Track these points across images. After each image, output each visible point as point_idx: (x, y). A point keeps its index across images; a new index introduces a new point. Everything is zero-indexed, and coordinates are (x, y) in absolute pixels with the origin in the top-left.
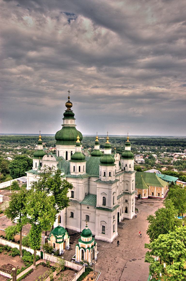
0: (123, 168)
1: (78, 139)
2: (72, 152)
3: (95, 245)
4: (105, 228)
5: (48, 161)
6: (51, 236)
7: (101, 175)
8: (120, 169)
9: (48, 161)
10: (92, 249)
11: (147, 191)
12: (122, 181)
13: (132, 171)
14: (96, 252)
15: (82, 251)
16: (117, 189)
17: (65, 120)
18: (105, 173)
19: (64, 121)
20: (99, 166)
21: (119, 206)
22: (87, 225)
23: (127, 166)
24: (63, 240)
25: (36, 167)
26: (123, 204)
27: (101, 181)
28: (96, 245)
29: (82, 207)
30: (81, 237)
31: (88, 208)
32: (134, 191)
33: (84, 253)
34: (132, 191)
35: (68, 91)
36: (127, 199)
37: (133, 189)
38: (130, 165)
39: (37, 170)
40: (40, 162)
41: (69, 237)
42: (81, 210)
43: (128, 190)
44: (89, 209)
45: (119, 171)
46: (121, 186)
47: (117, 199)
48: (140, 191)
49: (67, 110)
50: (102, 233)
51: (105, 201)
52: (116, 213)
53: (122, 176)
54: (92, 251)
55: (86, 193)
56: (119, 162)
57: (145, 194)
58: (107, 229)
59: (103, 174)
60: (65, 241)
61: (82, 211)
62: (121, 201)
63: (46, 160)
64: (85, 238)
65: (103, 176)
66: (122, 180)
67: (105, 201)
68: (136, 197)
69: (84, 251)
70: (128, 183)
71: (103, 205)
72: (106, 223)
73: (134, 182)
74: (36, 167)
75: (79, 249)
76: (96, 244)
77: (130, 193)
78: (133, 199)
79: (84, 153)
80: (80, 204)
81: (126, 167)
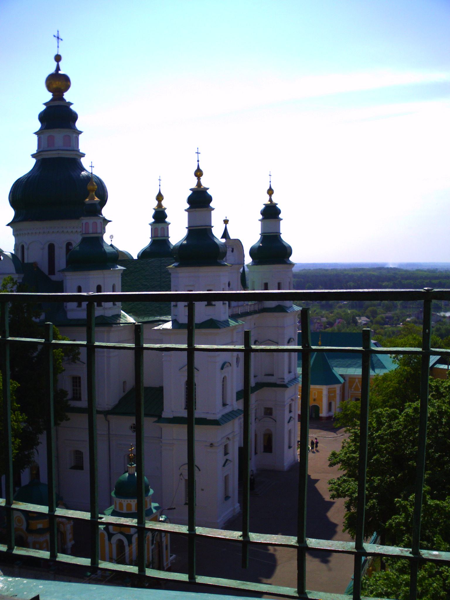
11: (338, 391)
14: (167, 549)
15: (120, 542)
26: (255, 423)
33: (127, 549)
35: (56, 34)
37: (290, 372)
43: (273, 375)
47: (237, 400)
49: (52, 100)
54: (155, 542)
57: (330, 405)
58: (203, 490)
64: (129, 500)
75: (110, 539)
77: (279, 382)
78: (290, 405)
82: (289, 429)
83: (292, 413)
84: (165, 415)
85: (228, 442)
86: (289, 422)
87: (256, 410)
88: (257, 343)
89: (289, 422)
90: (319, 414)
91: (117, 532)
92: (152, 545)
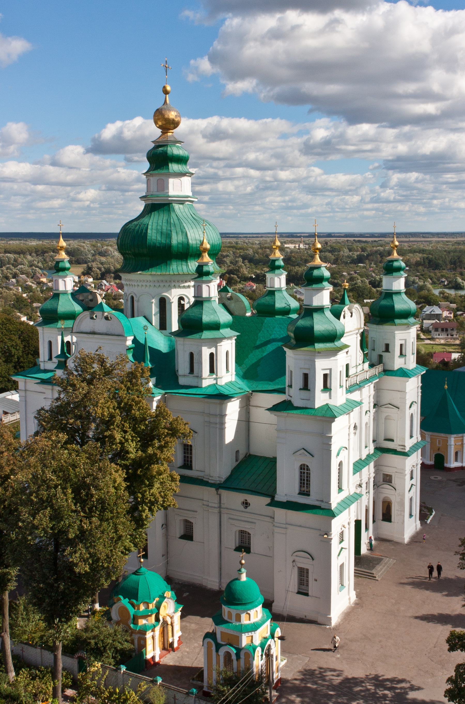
0: (375, 359)
1: (205, 250)
2: (181, 299)
3: (273, 636)
4: (307, 577)
5: (94, 333)
6: (115, 603)
7: (290, 386)
8: (363, 362)
9: (94, 333)
10: (263, 651)
12: (369, 407)
13: (411, 368)
15: (228, 655)
16: (352, 435)
17: (153, 180)
18: (306, 377)
19: (148, 182)
20: (285, 352)
21: (360, 495)
22: (242, 564)
23: (390, 349)
24: (157, 620)
25: (50, 359)
27: (292, 405)
28: (276, 635)
29: (222, 502)
30: (223, 606)
31: (247, 503)
32: (416, 442)
34: (409, 443)
36: (388, 471)
37: (411, 437)
38: (401, 345)
39: (56, 368)
40: (65, 341)
41: (180, 609)
42: (220, 513)
43: (392, 440)
44: (249, 509)
45: (360, 368)
46: (366, 424)
47: (354, 474)
48: (439, 441)
50: (299, 593)
51: (308, 481)
52: (349, 524)
53: (372, 386)
55: (237, 452)
56: (359, 335)
57: (456, 453)
58: (316, 580)
59: (298, 382)
60: (165, 623)
61: (222, 515)
62: (369, 479)
63: (88, 330)
65: (300, 389)
66: (372, 405)
67: (307, 480)
68: (423, 465)
69: (234, 657)
70: (392, 412)
71: (300, 494)
72: (313, 559)
73: (416, 410)
74: (50, 359)
75: (217, 651)
76: (278, 633)
77: (399, 449)
78: (412, 472)
79: (227, 302)
80: (217, 489)
81: (385, 355)
82: (410, 497)
83: (413, 479)
84: (278, 498)
85: (343, 528)
86: (409, 491)
87: (374, 478)
88: (377, 406)
89: (409, 491)
90: (444, 463)
91: (225, 643)
92: (261, 660)
